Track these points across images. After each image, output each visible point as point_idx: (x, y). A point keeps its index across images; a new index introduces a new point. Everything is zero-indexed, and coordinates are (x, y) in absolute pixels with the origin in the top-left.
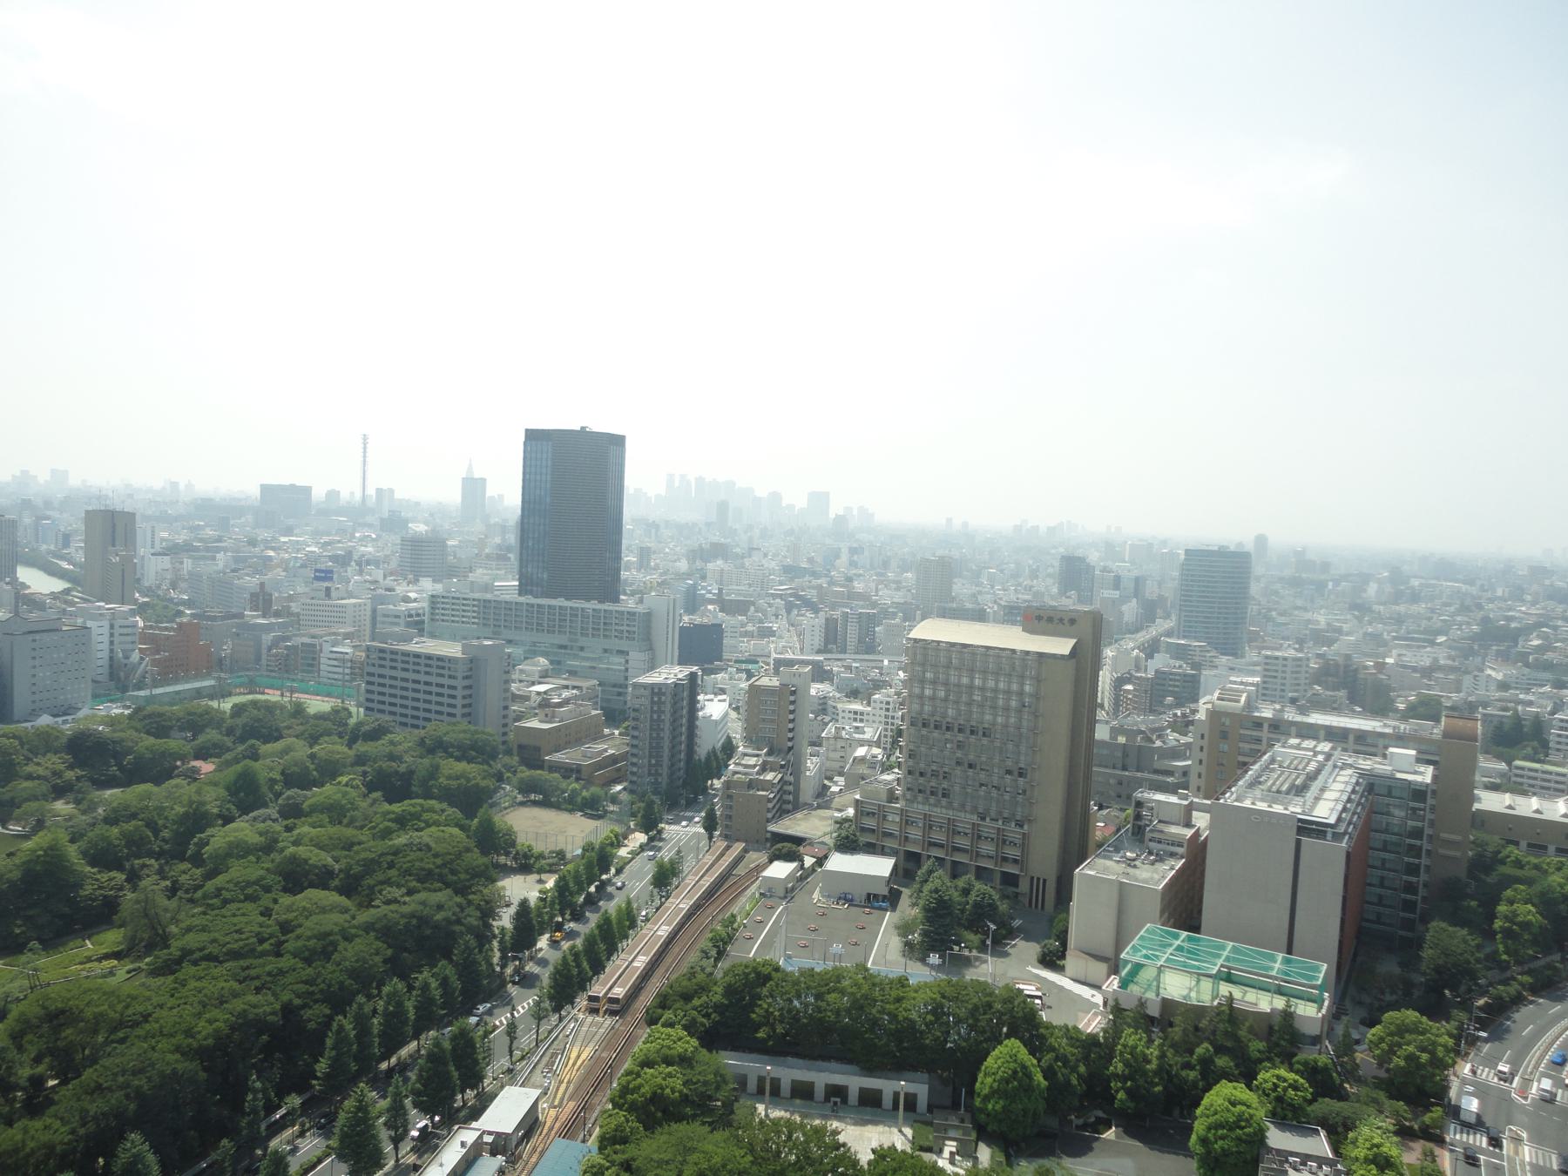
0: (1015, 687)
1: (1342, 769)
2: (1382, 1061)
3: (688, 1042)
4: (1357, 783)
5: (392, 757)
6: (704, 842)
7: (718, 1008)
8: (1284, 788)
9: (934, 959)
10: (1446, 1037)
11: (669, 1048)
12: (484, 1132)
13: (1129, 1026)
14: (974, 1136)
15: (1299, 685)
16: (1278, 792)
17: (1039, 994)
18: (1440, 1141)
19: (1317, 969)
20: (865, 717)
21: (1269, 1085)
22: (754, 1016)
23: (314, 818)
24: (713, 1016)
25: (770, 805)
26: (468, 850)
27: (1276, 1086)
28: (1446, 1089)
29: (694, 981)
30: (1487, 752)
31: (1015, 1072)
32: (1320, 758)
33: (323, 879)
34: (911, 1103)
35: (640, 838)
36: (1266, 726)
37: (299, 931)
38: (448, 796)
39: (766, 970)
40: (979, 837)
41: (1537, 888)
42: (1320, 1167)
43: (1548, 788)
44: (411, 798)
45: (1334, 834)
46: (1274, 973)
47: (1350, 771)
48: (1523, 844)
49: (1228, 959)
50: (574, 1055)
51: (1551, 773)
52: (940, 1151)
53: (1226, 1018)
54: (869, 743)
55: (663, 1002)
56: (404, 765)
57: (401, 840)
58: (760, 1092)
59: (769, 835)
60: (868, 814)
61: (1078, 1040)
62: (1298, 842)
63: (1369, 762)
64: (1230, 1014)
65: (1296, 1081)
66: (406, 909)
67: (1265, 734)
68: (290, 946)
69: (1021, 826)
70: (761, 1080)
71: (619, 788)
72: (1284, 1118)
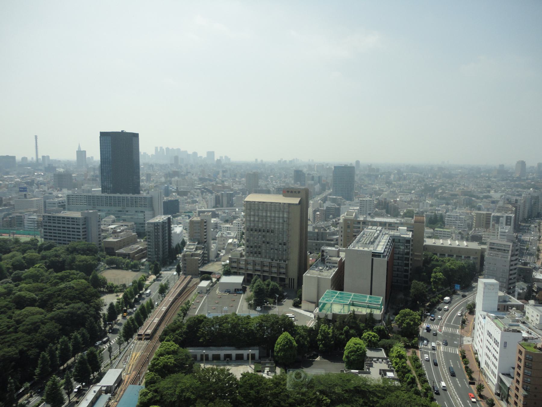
0: (281, 215)
2: (400, 325)
3: (175, 346)
4: (390, 239)
5: (56, 256)
6: (177, 276)
7: (185, 333)
8: (368, 242)
9: (259, 308)
10: (418, 316)
11: (169, 349)
12: (102, 386)
13: (323, 323)
14: (274, 365)
16: (366, 244)
17: (294, 316)
18: (417, 348)
19: (379, 299)
20: (231, 229)
21: (366, 337)
22: (198, 334)
23: (27, 281)
24: (184, 336)
25: (200, 262)
26: (88, 287)
27: (368, 337)
28: (418, 332)
29: (176, 325)
30: (427, 226)
31: (287, 342)
32: (378, 232)
33: (32, 302)
34: (253, 356)
35: (153, 277)
36: (361, 223)
37: (24, 323)
38: (79, 268)
39: (202, 318)
40: (272, 267)
41: (443, 268)
42: (382, 361)
43: (445, 236)
44: (65, 270)
45: (383, 256)
46: (367, 302)
47: (387, 236)
48: (438, 254)
49: (352, 299)
50: (134, 355)
51: (446, 232)
52: (264, 371)
53: (352, 317)
54: (233, 238)
55: (165, 333)
56: (61, 258)
57: (62, 286)
58: (202, 360)
59: (200, 272)
60: (234, 262)
61: (306, 330)
62: (372, 260)
64: (354, 316)
65: (374, 335)
66: (66, 311)
67: (361, 225)
68: (21, 329)
69: (285, 262)
70: (202, 355)
71: (144, 260)
72: (371, 347)
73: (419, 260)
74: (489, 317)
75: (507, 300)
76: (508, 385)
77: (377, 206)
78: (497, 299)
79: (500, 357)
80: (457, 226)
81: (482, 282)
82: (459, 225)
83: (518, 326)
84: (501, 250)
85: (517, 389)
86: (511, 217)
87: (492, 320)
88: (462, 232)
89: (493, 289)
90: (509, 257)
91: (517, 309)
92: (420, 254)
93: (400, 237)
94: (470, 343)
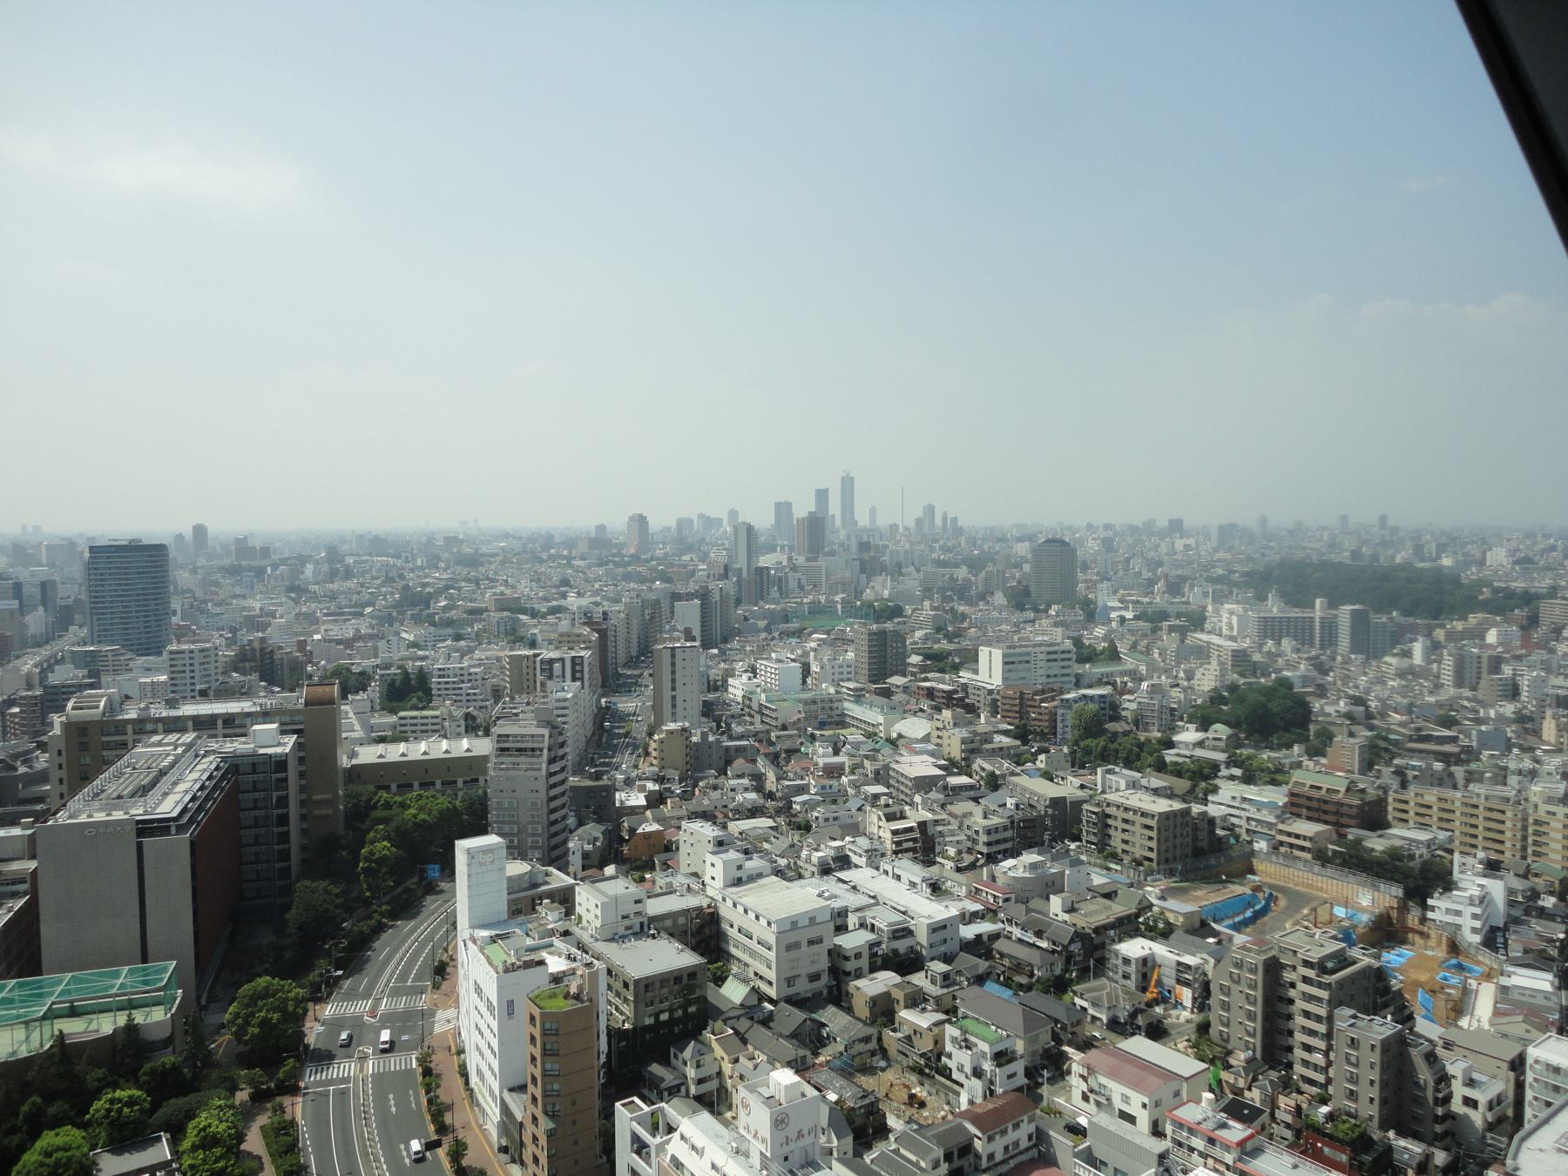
1: (204, 756)
2: (238, 1036)
4: (217, 768)
15: (209, 675)
16: (119, 797)
27: (109, 1111)
28: (302, 1035)
30: (383, 709)
32: (180, 750)
41: (393, 824)
43: (427, 731)
46: (114, 991)
48: (394, 787)
62: (140, 846)
63: (236, 744)
65: (130, 1097)
73: (326, 816)
74: (474, 942)
75: (540, 881)
76: (519, 1116)
77: (238, 664)
78: (505, 885)
79: (501, 1044)
80: (464, 698)
81: (464, 847)
82: (468, 694)
83: (552, 945)
84: (526, 750)
85: (535, 1119)
86: (582, 657)
87: (482, 950)
88: (475, 713)
89: (492, 862)
90: (544, 766)
91: (553, 902)
92: (328, 796)
93: (255, 755)
94: (451, 1026)
